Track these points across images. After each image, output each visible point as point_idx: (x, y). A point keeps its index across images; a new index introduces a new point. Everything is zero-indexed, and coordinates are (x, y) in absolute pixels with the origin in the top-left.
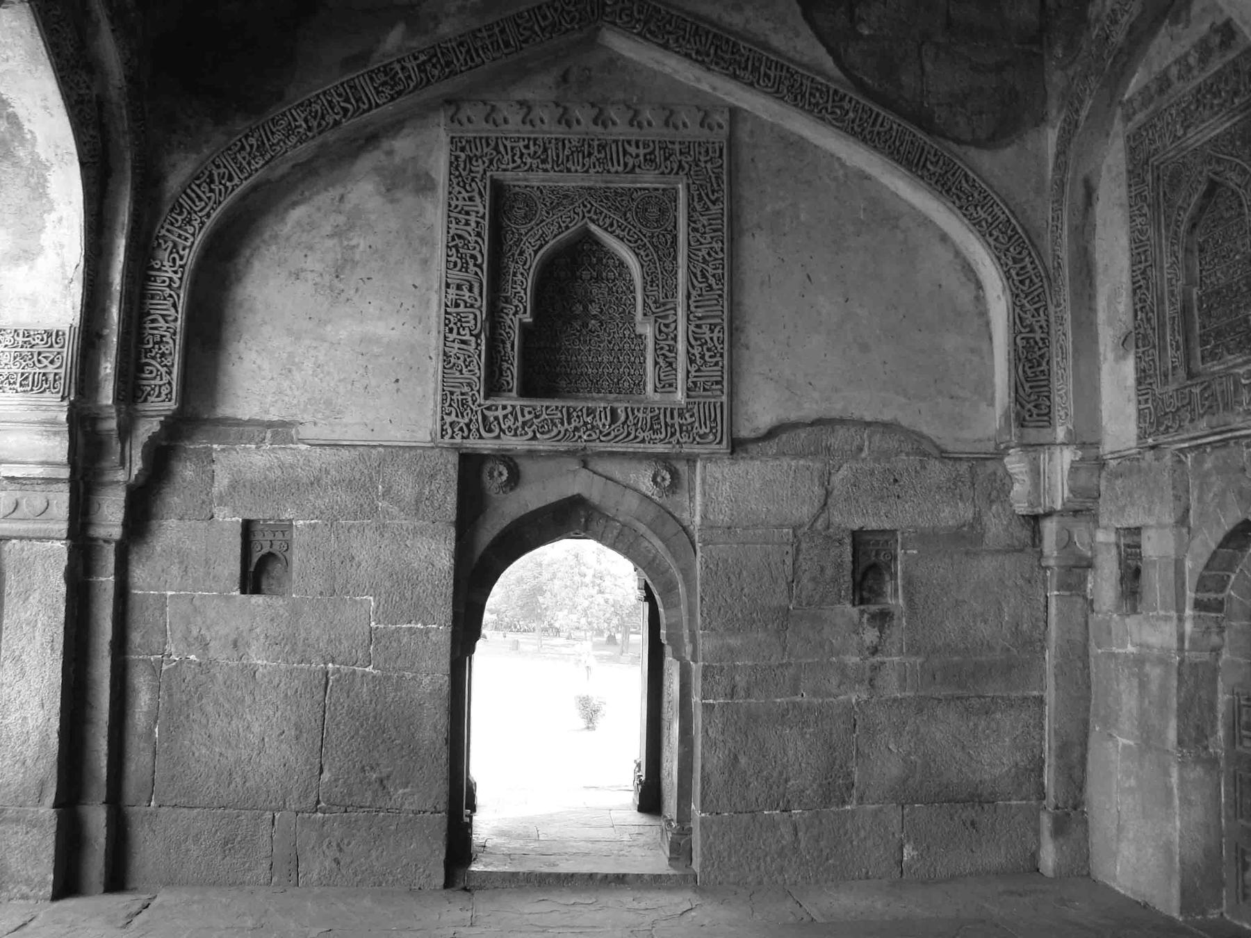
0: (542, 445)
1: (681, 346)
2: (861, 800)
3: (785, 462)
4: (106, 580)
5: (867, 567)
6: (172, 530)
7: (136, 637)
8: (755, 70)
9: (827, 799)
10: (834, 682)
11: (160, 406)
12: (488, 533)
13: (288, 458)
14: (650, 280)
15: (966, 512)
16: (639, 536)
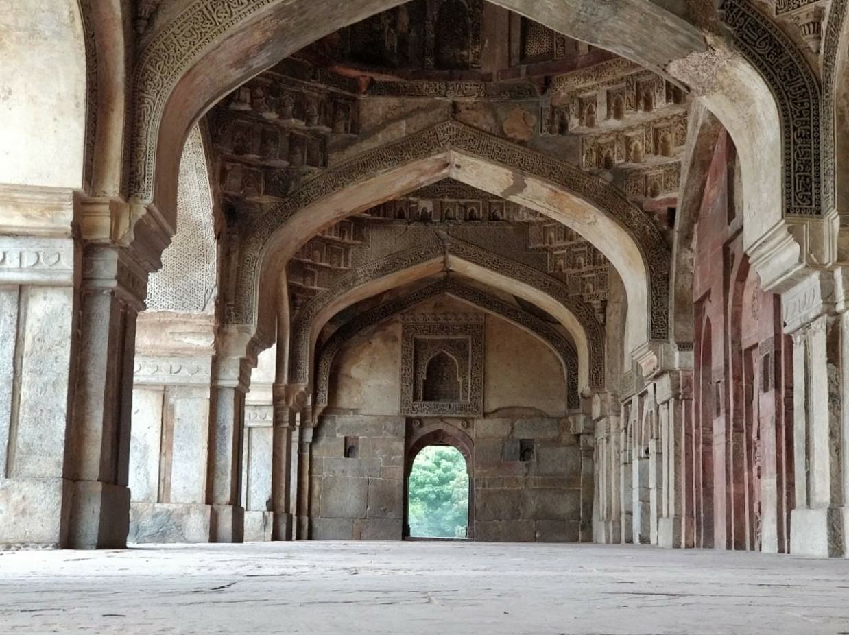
0: (430, 415)
1: (469, 386)
2: (523, 518)
3: (500, 419)
4: (307, 454)
5: (525, 450)
6: (323, 441)
7: (314, 470)
8: (491, 304)
9: (513, 518)
10: (515, 482)
11: (323, 405)
12: (414, 440)
13: (357, 419)
14: (461, 366)
15: (556, 434)
16: (458, 441)
